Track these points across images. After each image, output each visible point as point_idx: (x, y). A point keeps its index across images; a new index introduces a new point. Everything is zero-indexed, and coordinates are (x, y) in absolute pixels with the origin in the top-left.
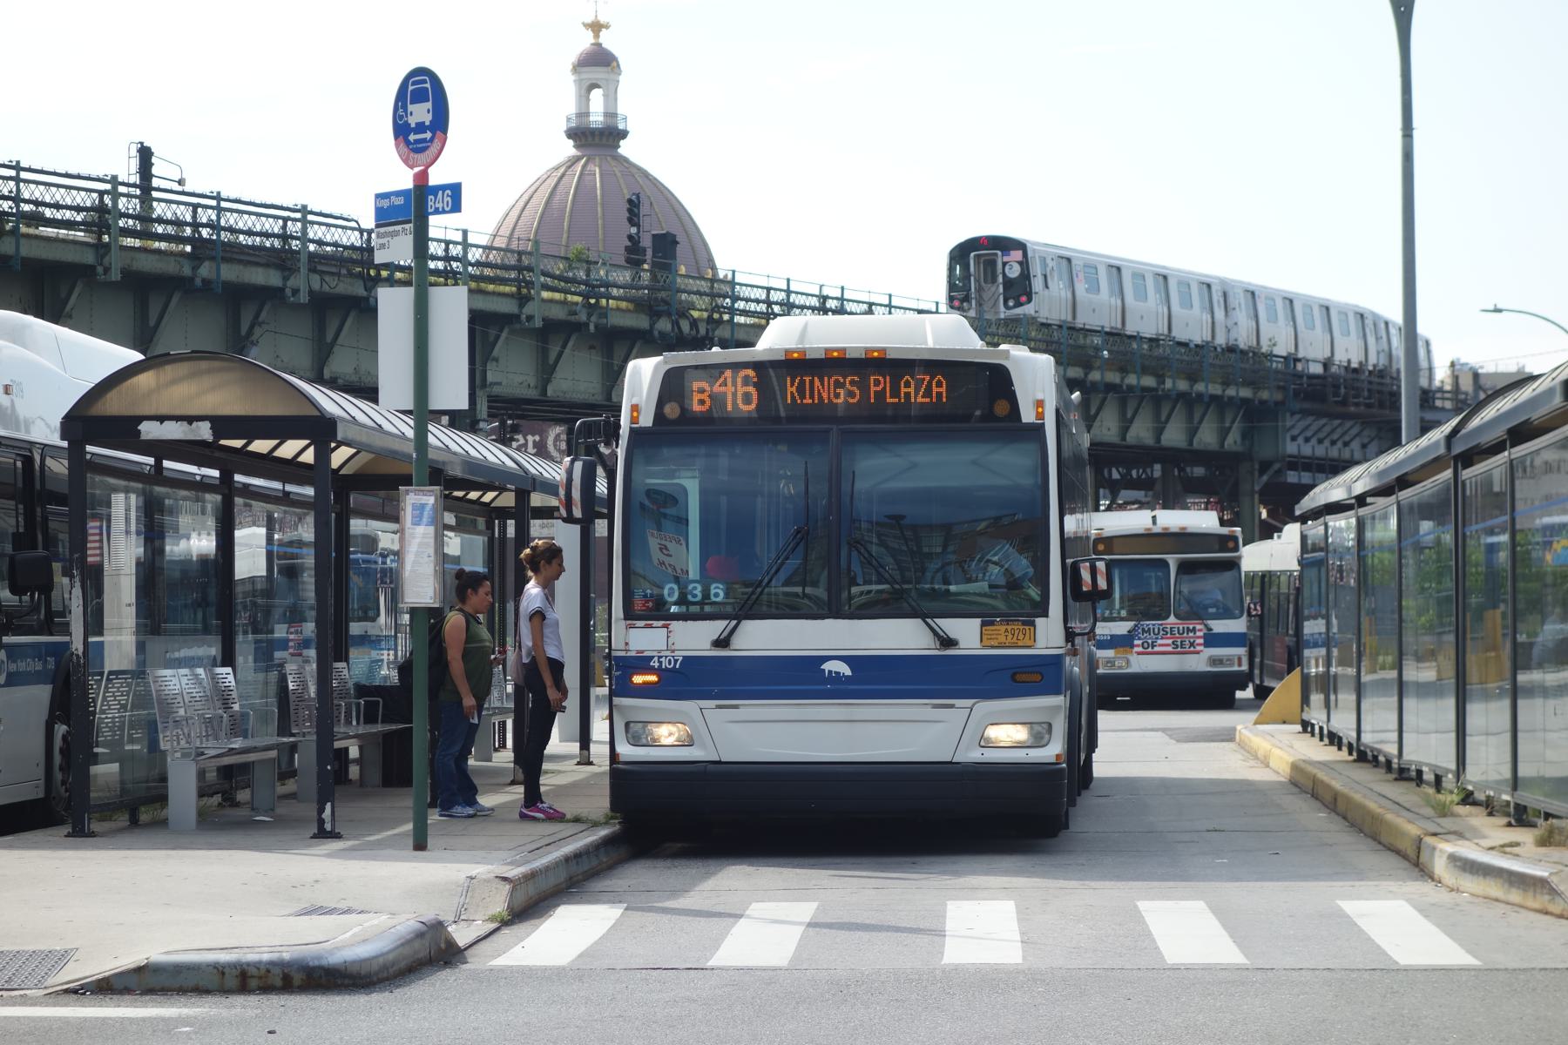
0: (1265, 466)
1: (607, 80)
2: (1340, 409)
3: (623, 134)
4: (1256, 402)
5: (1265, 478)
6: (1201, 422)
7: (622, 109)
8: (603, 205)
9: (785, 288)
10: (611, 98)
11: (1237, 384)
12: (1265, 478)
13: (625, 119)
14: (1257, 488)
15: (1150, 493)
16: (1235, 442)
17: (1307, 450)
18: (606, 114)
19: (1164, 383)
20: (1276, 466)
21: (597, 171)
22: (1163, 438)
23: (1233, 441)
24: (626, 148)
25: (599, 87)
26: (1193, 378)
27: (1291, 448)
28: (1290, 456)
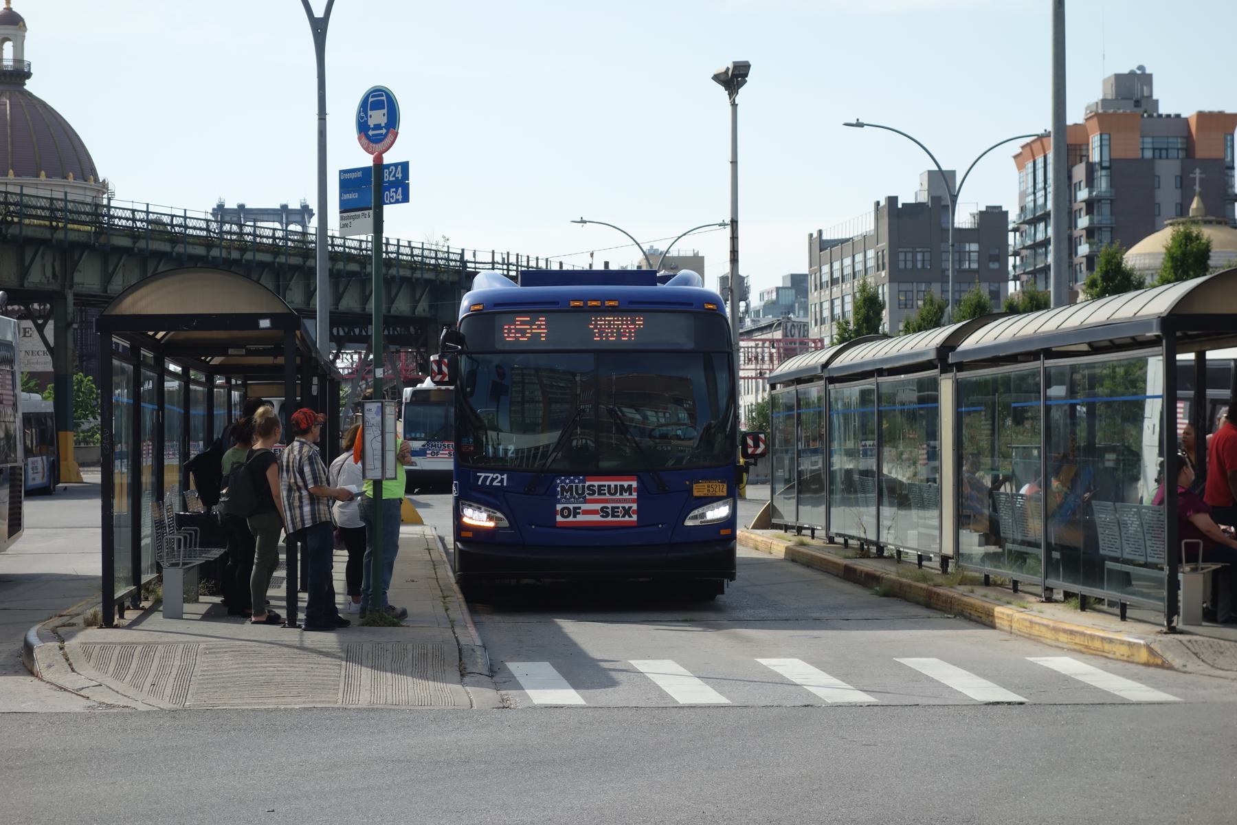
1: (16, 35)
3: (28, 75)
6: (396, 295)
7: (27, 58)
8: (11, 127)
9: (63, 197)
10: (19, 49)
13: (29, 65)
16: (424, 310)
18: (15, 60)
19: (365, 268)
21: (8, 102)
22: (367, 307)
23: (422, 308)
24: (30, 85)
25: (9, 40)
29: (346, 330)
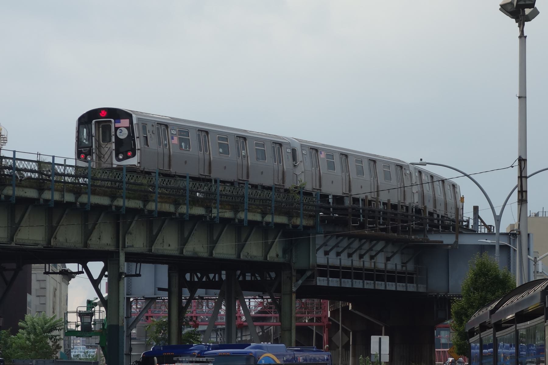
0: (301, 272)
2: (356, 232)
4: (291, 227)
5: (300, 282)
6: (246, 240)
11: (272, 214)
12: (300, 282)
14: (294, 289)
15: (218, 291)
16: (277, 255)
17: (333, 260)
20: (309, 273)
22: (214, 252)
26: (236, 209)
27: (321, 259)
28: (319, 266)
29: (199, 275)
